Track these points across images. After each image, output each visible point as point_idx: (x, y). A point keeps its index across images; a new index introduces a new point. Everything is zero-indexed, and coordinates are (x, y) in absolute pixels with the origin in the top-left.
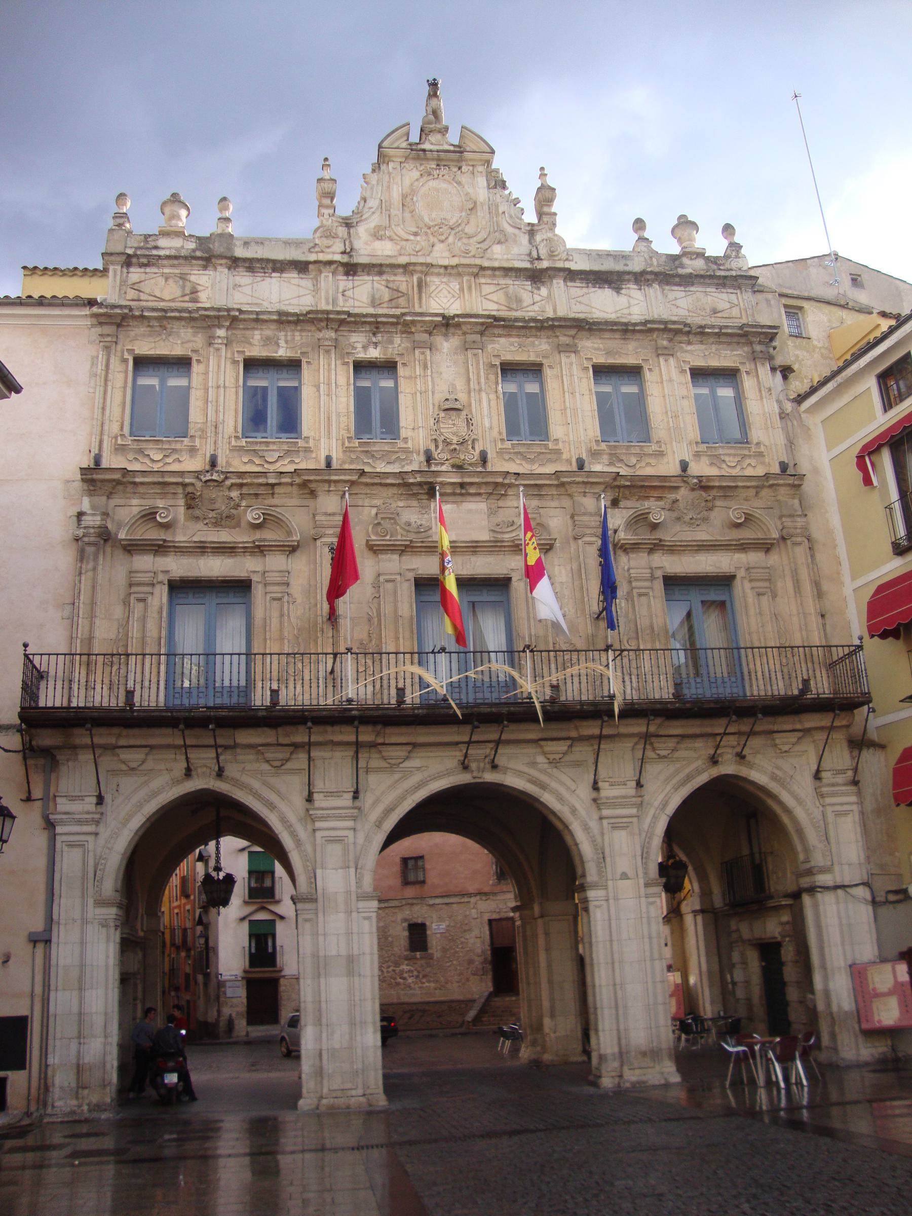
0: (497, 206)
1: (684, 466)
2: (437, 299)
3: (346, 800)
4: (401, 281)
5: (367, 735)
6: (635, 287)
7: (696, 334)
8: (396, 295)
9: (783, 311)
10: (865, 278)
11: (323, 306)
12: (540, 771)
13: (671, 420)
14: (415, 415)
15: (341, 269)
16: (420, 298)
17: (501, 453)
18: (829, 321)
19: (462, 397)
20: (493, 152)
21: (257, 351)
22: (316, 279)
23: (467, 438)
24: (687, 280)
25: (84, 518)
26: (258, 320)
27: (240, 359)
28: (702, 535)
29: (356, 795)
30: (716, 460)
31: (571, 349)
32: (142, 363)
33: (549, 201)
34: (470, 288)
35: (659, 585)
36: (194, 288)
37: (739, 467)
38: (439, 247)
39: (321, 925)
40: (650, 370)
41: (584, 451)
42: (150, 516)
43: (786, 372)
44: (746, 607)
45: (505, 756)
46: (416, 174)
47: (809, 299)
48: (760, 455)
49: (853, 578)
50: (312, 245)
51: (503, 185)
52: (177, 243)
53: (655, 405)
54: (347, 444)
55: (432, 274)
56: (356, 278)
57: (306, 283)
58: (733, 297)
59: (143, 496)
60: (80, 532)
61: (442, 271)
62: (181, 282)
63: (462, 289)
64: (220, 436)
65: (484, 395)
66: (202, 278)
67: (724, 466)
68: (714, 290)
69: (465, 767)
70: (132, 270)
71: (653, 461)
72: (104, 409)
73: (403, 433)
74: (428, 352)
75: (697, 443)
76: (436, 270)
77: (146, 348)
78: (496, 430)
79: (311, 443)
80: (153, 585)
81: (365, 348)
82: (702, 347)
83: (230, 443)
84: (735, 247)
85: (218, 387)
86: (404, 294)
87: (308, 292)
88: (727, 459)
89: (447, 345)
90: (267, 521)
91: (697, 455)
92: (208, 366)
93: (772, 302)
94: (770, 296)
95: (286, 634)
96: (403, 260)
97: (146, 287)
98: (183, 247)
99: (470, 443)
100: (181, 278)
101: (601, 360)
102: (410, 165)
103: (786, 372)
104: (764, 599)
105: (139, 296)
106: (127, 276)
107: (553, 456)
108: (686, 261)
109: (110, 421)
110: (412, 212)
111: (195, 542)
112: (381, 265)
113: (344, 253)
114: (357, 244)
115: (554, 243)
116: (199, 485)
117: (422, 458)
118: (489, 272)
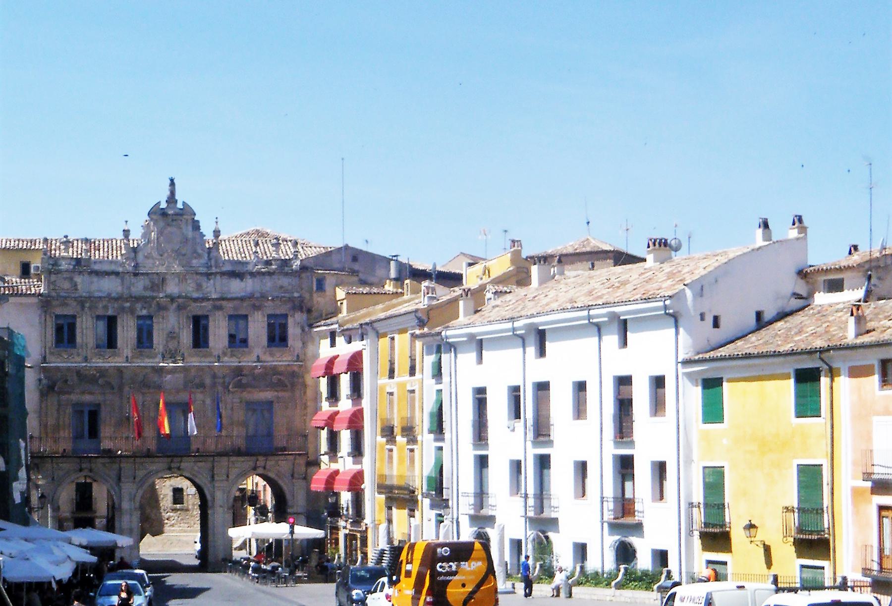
1: (258, 356)
3: (131, 479)
10: (360, 257)
19: (177, 330)
20: (195, 214)
31: (220, 308)
43: (309, 311)
57: (119, 280)
66: (78, 279)
81: (141, 310)
101: (232, 313)
115: (218, 259)
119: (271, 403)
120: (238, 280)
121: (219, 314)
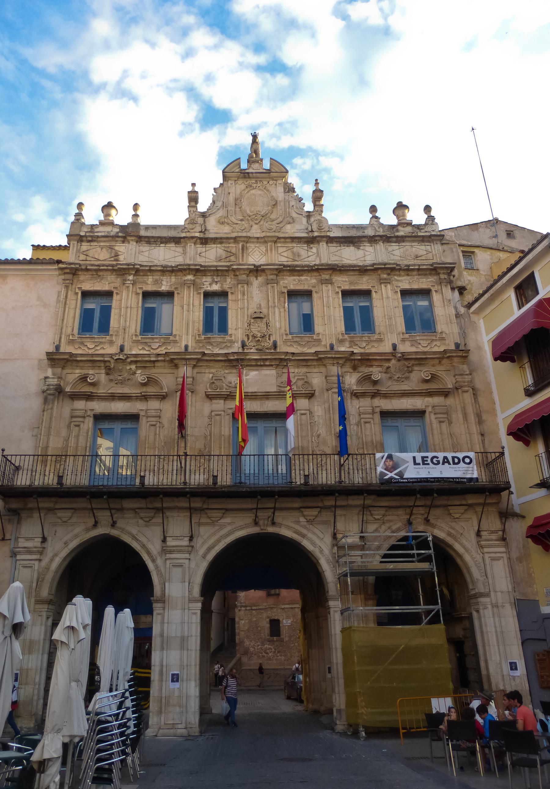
0: (289, 202)
1: (394, 347)
2: (252, 256)
3: (185, 542)
4: (233, 247)
5: (197, 503)
6: (369, 245)
7: (404, 270)
8: (229, 254)
9: (461, 254)
11: (188, 262)
12: (301, 526)
13: (387, 321)
14: (237, 321)
15: (198, 241)
16: (243, 256)
17: (286, 341)
18: (491, 259)
19: (265, 311)
21: (150, 288)
22: (184, 247)
23: (266, 333)
24: (400, 239)
25: (47, 380)
26: (150, 270)
27: (140, 292)
28: (405, 387)
29: (191, 538)
30: (414, 343)
31: (329, 282)
32: (86, 294)
33: (320, 198)
34: (271, 249)
35: (377, 417)
36: (117, 253)
37: (429, 347)
38: (255, 227)
39: (166, 617)
40: (376, 292)
41: (334, 339)
42: (84, 379)
43: (462, 290)
44: (432, 430)
45: (279, 517)
46: (243, 187)
47: (478, 247)
48: (443, 339)
49: (502, 412)
50: (183, 228)
51: (293, 190)
52: (108, 229)
53: (378, 313)
54: (197, 338)
55: (250, 242)
56: (207, 246)
57: (179, 249)
58: (429, 247)
59: (82, 368)
60: (45, 388)
61: (255, 240)
62: (110, 250)
63: (267, 250)
64: (127, 334)
65: (277, 309)
66: (121, 248)
67: (420, 346)
68: (417, 244)
69: (256, 523)
70: (83, 244)
71: (376, 345)
72: (63, 320)
73: (230, 332)
74: (246, 286)
75: (403, 333)
76: (252, 240)
77: (88, 286)
78: (283, 329)
79: (177, 338)
80: (84, 417)
81: (211, 284)
82: (409, 278)
83: (132, 338)
84: (431, 219)
85: (127, 307)
86: (234, 254)
87: (180, 254)
88: (421, 342)
89: (256, 282)
90: (150, 381)
91: (403, 340)
92: (122, 296)
93: (454, 250)
94: (452, 246)
95: (157, 445)
96: (234, 235)
97: (91, 253)
98: (112, 231)
99: (267, 336)
100: (110, 248)
101: (347, 287)
102: (240, 182)
103: (462, 290)
104: (444, 426)
105: (86, 258)
106: (80, 248)
107: (316, 343)
108: (400, 228)
109: (67, 327)
110: (240, 208)
111: (109, 393)
112: (221, 238)
113: (201, 232)
114: (209, 227)
115: (322, 222)
116: (112, 361)
117: (240, 344)
118: (283, 240)
119: (420, 414)
120: (352, 248)
121: (327, 290)
